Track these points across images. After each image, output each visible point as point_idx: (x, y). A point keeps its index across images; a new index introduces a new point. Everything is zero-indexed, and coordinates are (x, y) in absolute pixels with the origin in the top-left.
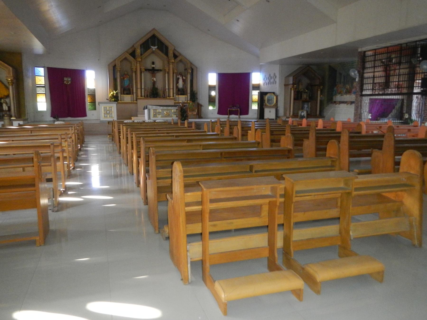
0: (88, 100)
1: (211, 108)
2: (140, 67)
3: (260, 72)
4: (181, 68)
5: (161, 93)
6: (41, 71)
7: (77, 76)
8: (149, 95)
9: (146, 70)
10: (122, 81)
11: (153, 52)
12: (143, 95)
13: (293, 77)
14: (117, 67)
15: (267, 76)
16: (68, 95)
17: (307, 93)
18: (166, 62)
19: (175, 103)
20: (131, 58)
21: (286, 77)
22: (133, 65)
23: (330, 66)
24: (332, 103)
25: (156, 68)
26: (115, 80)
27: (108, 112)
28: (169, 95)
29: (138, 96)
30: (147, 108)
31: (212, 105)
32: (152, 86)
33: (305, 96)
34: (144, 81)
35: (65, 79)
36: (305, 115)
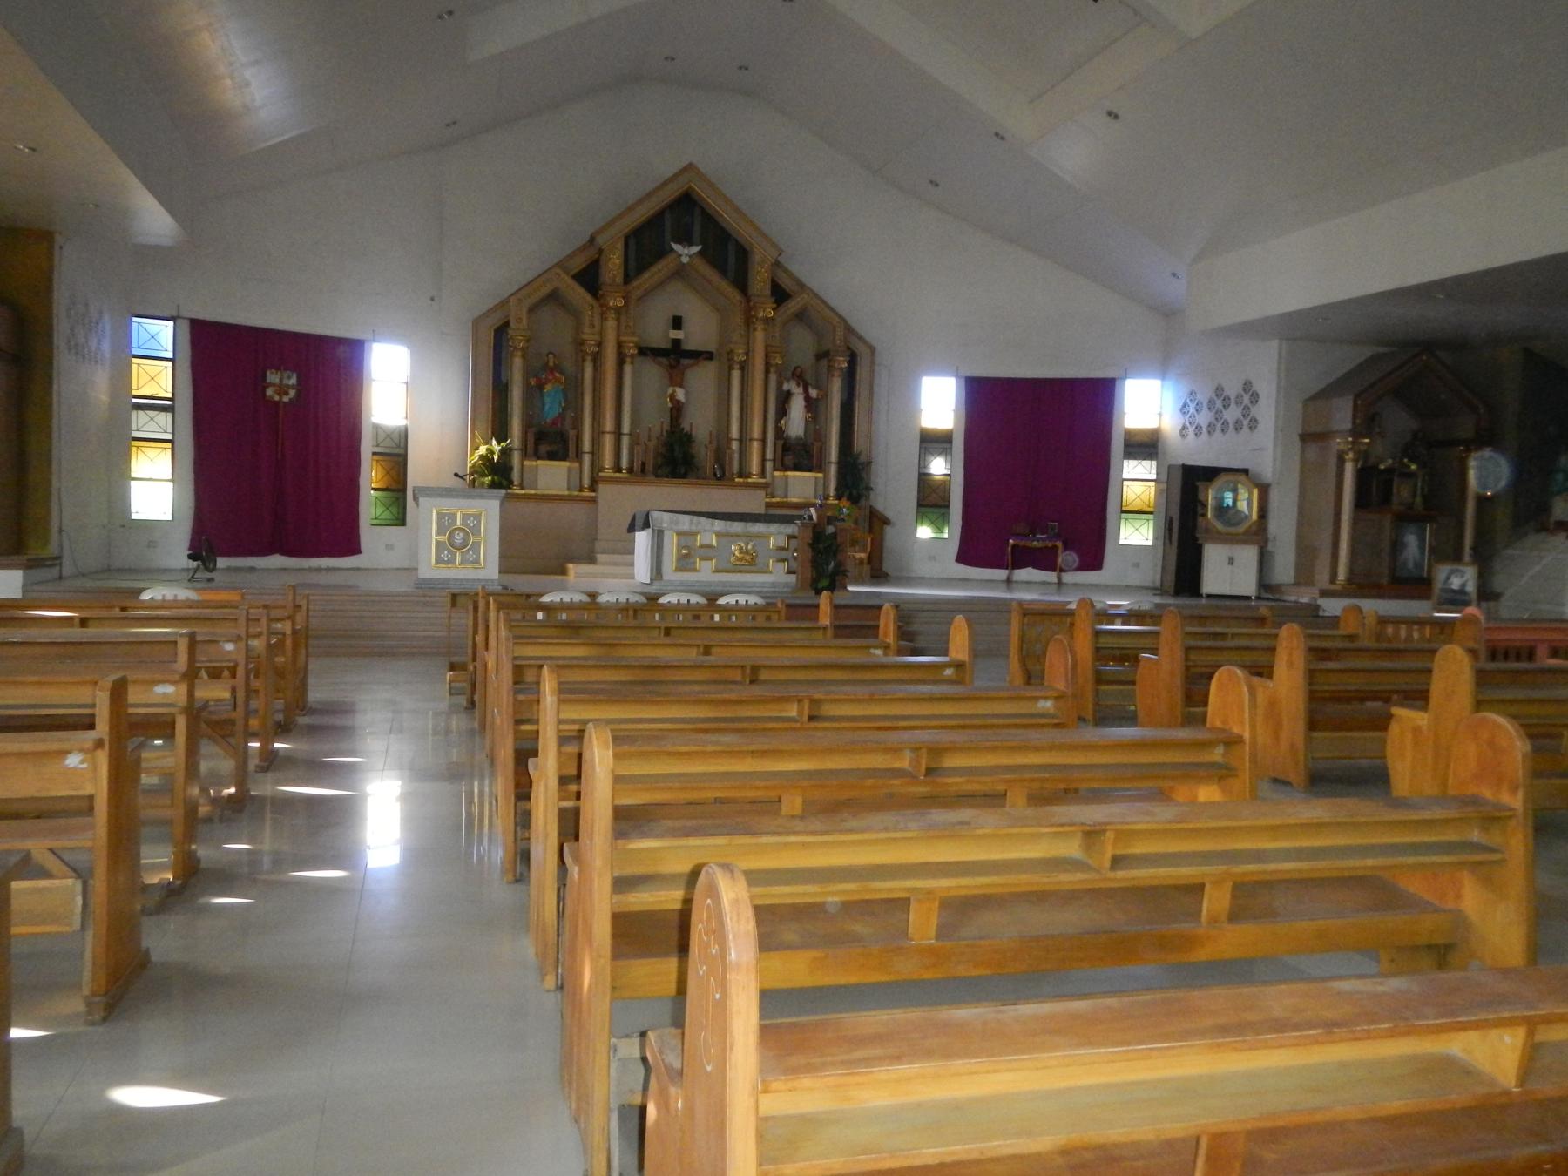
0: (371, 476)
1: (925, 532)
2: (619, 336)
3: (1163, 375)
4: (802, 346)
5: (703, 454)
6: (159, 334)
7: (329, 367)
8: (650, 467)
9: (644, 351)
10: (531, 398)
11: (680, 273)
12: (624, 463)
13: (1357, 397)
14: (511, 332)
15: (1203, 397)
16: (276, 447)
17: (1411, 475)
18: (738, 319)
19: (768, 505)
20: (578, 295)
21: (1314, 398)
22: (587, 330)
23: (1528, 353)
24: (1543, 528)
25: (690, 345)
26: (501, 391)
27: (458, 537)
28: (741, 468)
29: (602, 469)
30: (646, 525)
31: (933, 523)
32: (666, 427)
33: (1402, 492)
34: (632, 402)
35: (273, 377)
36: (1471, 588)
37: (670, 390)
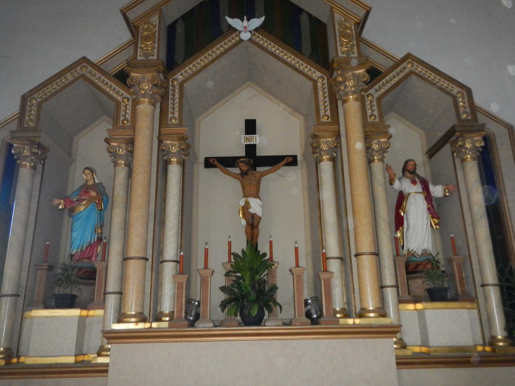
12: (167, 305)
37: (242, 203)
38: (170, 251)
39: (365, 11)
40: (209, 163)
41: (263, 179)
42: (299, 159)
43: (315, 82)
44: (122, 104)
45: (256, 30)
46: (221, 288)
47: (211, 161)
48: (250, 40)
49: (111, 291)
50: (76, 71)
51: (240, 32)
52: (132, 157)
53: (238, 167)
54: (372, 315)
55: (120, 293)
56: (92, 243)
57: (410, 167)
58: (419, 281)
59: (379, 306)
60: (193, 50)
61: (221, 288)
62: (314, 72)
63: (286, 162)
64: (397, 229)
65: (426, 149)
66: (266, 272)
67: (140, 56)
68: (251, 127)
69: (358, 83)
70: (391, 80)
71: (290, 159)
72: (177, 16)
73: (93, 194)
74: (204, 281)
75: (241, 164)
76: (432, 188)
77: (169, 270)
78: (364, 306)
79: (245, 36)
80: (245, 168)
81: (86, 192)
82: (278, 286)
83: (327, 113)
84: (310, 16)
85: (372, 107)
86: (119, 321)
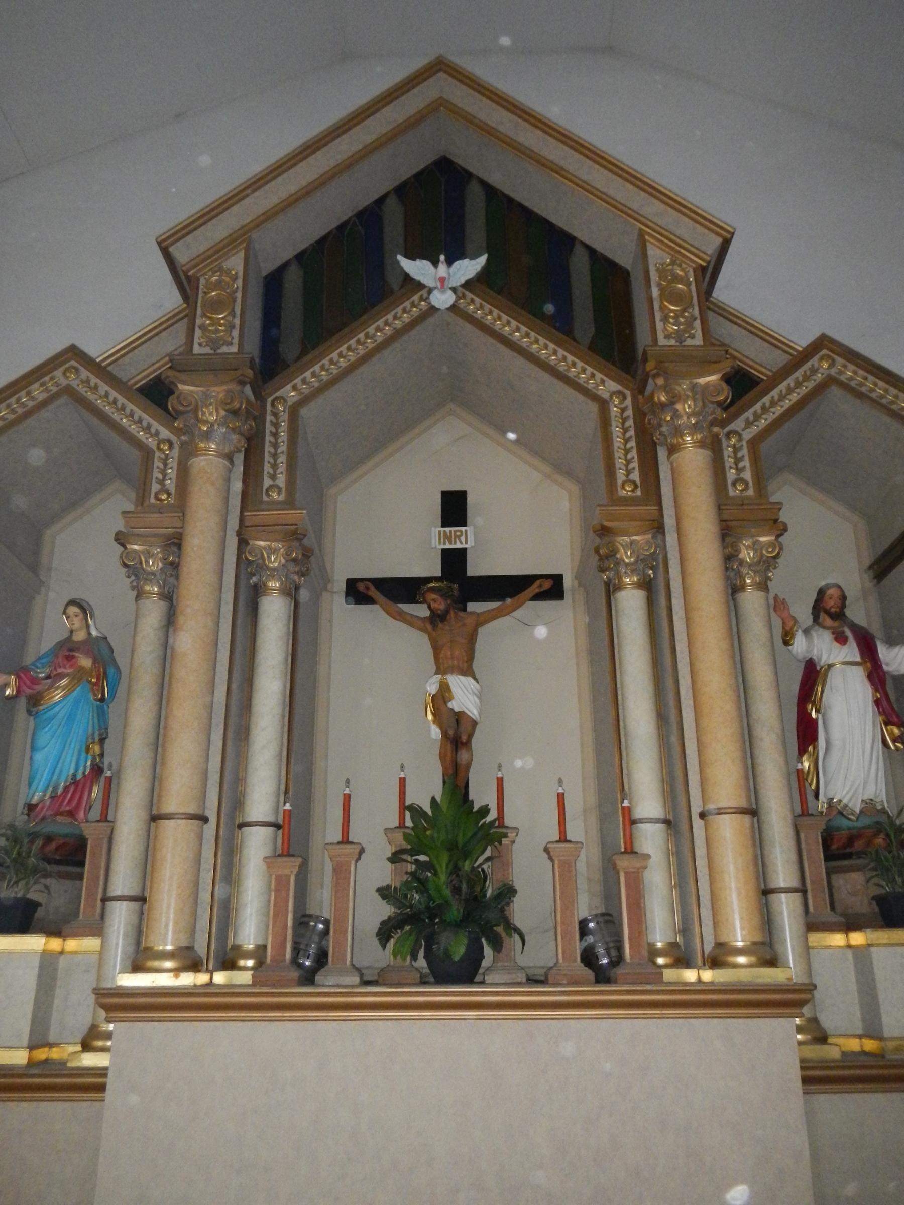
12: (250, 932)
37: (432, 688)
38: (262, 799)
39: (719, 240)
40: (358, 592)
41: (482, 630)
42: (567, 583)
43: (603, 405)
44: (157, 454)
45: (468, 285)
46: (379, 890)
47: (361, 587)
48: (453, 308)
49: (118, 893)
50: (52, 379)
51: (430, 291)
52: (177, 577)
53: (424, 601)
54: (742, 960)
55: (141, 899)
56: (79, 776)
57: (831, 603)
58: (857, 878)
59: (758, 938)
60: (321, 332)
61: (379, 890)
62: (603, 382)
63: (537, 591)
64: (802, 751)
65: (867, 562)
66: (488, 853)
67: (200, 345)
68: (454, 509)
69: (704, 406)
70: (782, 397)
71: (547, 585)
72: (288, 254)
73: (85, 662)
74: (341, 872)
75: (431, 596)
76: (883, 651)
77: (257, 845)
78: (723, 939)
79: (443, 299)
80: (440, 605)
81: (69, 658)
82: (517, 885)
83: (632, 477)
84: (592, 252)
85: (737, 461)
86: (137, 968)
